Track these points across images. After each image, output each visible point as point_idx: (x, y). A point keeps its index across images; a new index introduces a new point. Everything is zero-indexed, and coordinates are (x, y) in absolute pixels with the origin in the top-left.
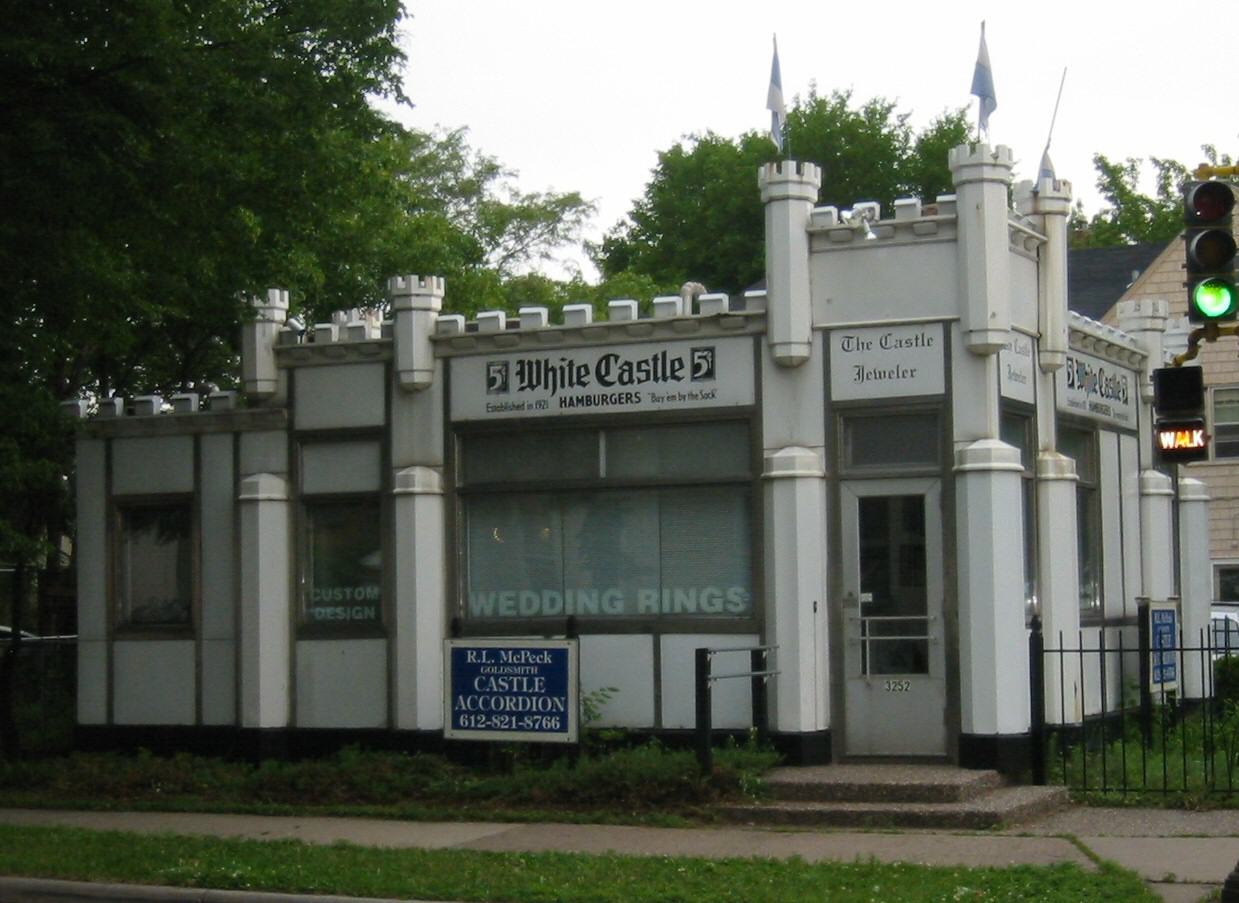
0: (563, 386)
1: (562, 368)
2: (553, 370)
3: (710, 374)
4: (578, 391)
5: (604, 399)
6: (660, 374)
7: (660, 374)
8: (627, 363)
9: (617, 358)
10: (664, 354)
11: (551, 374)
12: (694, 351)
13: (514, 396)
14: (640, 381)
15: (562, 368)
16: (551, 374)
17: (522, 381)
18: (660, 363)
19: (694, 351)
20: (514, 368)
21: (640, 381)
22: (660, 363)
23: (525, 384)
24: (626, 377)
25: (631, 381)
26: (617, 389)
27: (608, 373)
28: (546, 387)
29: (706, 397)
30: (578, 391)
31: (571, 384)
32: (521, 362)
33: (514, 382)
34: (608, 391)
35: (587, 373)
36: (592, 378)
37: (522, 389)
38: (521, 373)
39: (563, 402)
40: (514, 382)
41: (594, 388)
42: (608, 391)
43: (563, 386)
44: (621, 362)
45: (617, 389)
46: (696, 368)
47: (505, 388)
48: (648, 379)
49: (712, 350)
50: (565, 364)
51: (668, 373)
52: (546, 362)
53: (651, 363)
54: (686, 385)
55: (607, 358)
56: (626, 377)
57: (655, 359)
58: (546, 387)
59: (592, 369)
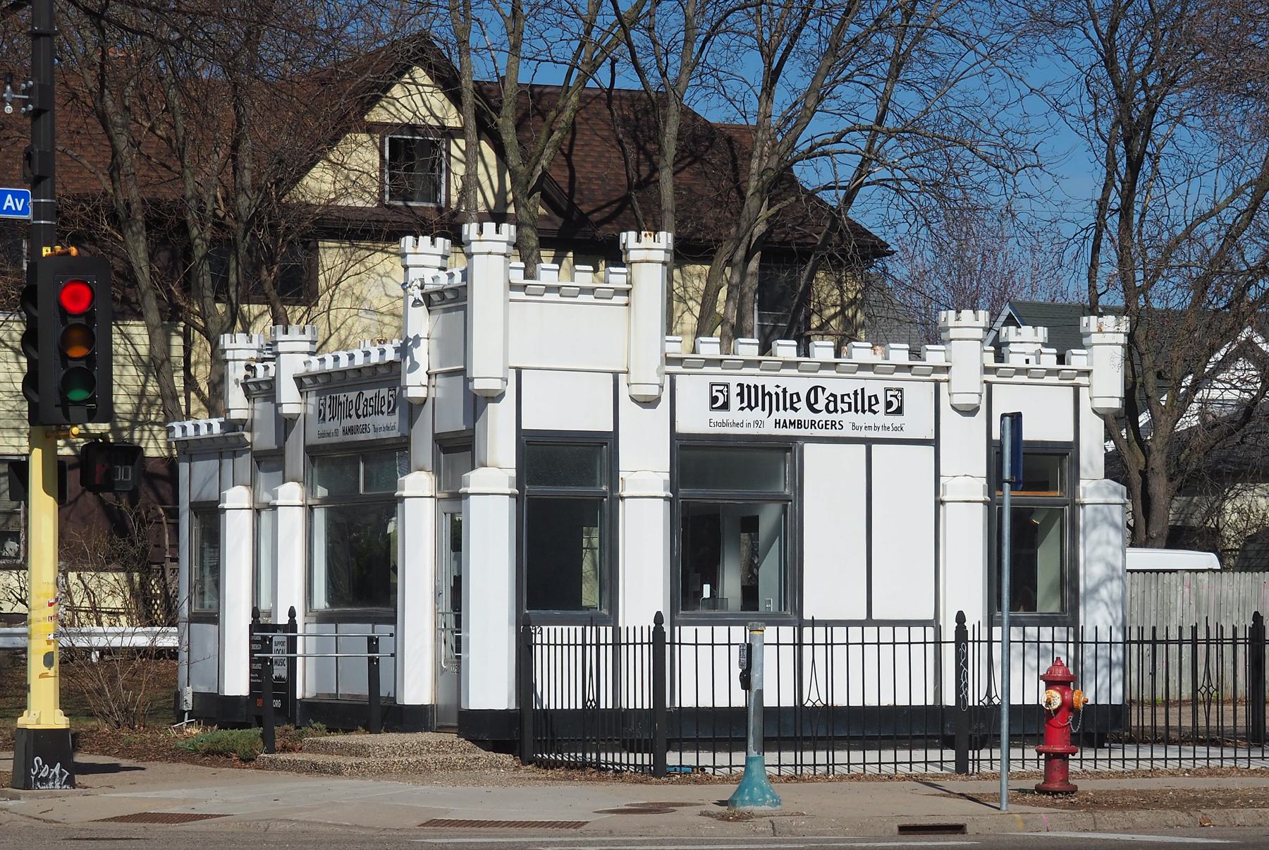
0: (778, 409)
1: (777, 394)
2: (769, 394)
3: (899, 411)
4: (790, 415)
5: (813, 423)
6: (859, 407)
7: (859, 407)
8: (832, 395)
9: (824, 389)
10: (863, 390)
11: (767, 398)
12: (887, 390)
13: (734, 414)
14: (843, 411)
15: (777, 394)
16: (767, 398)
17: (742, 402)
18: (859, 397)
19: (887, 390)
20: (735, 390)
21: (843, 411)
22: (859, 397)
23: (745, 404)
24: (831, 407)
25: (836, 410)
26: (824, 416)
27: (816, 402)
28: (763, 409)
29: (896, 429)
30: (790, 415)
31: (785, 409)
32: (741, 385)
33: (735, 402)
34: (816, 417)
35: (799, 400)
36: (802, 405)
37: (742, 409)
38: (741, 394)
39: (777, 423)
40: (735, 402)
41: (804, 414)
42: (816, 417)
43: (778, 409)
44: (827, 393)
45: (824, 416)
46: (889, 404)
47: (725, 406)
48: (850, 410)
49: (901, 390)
50: (780, 391)
51: (866, 407)
52: (763, 387)
53: (852, 396)
54: (881, 418)
55: (815, 388)
56: (831, 407)
57: (856, 393)
58: (763, 409)
59: (803, 398)
